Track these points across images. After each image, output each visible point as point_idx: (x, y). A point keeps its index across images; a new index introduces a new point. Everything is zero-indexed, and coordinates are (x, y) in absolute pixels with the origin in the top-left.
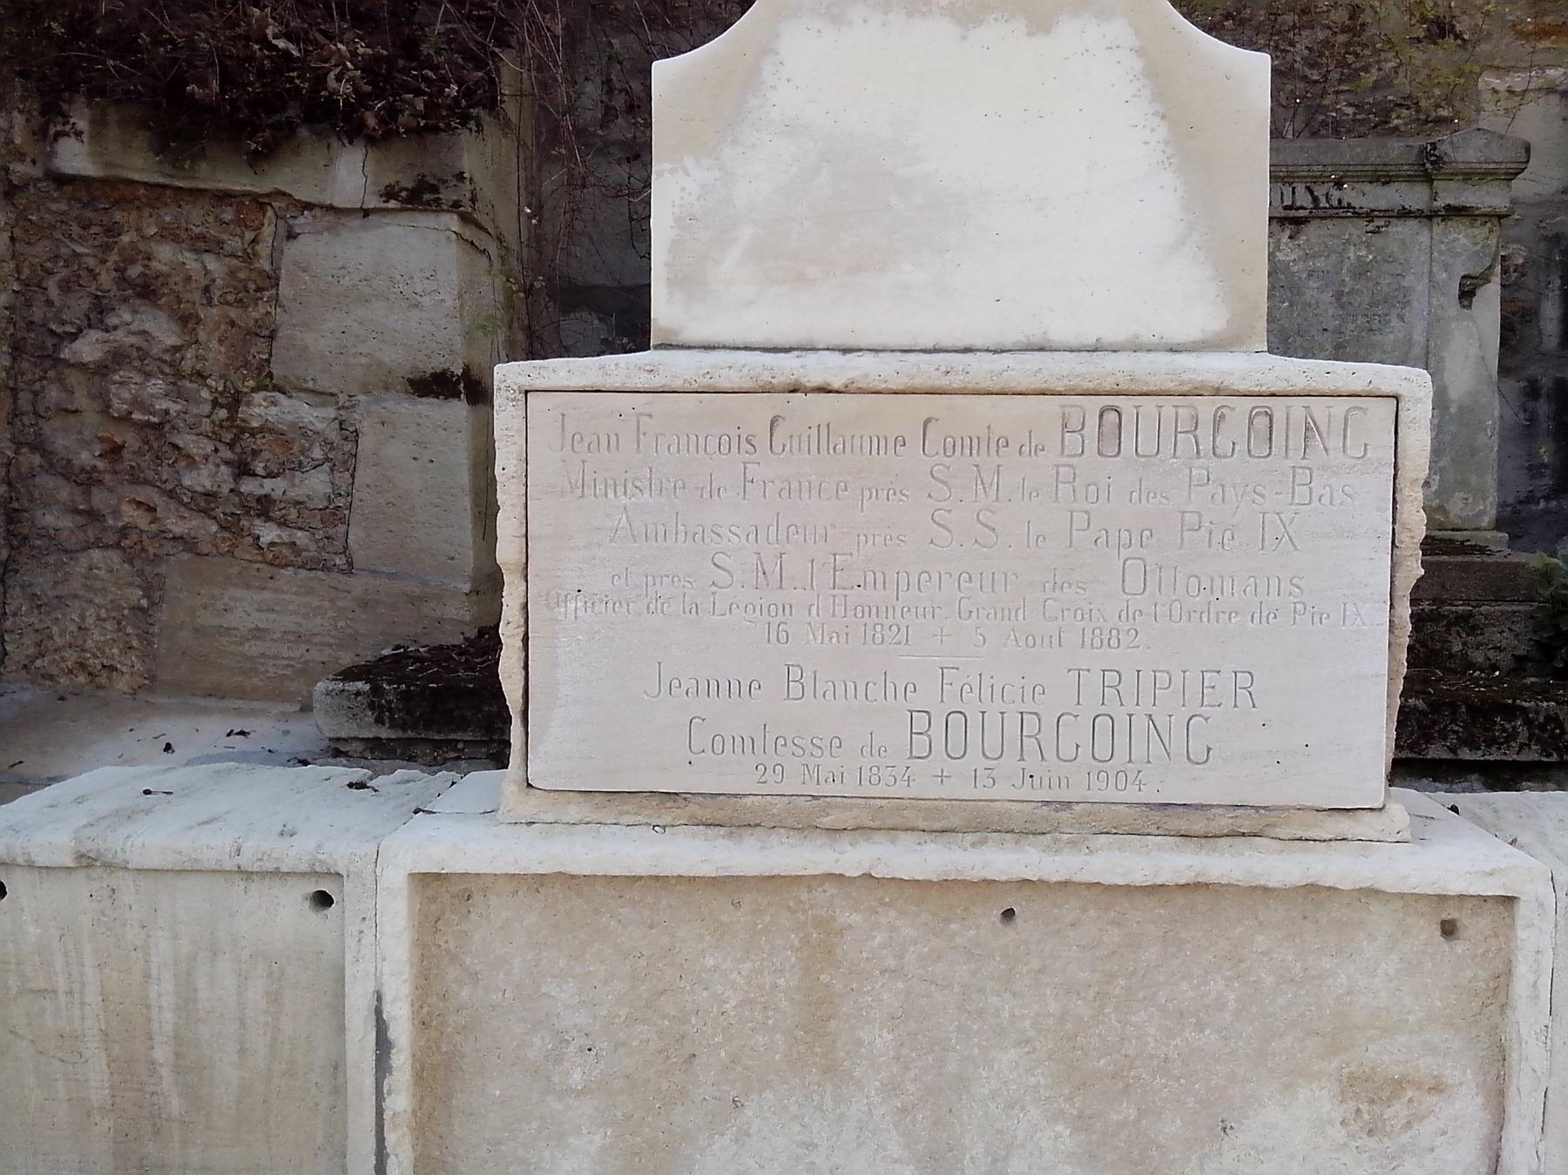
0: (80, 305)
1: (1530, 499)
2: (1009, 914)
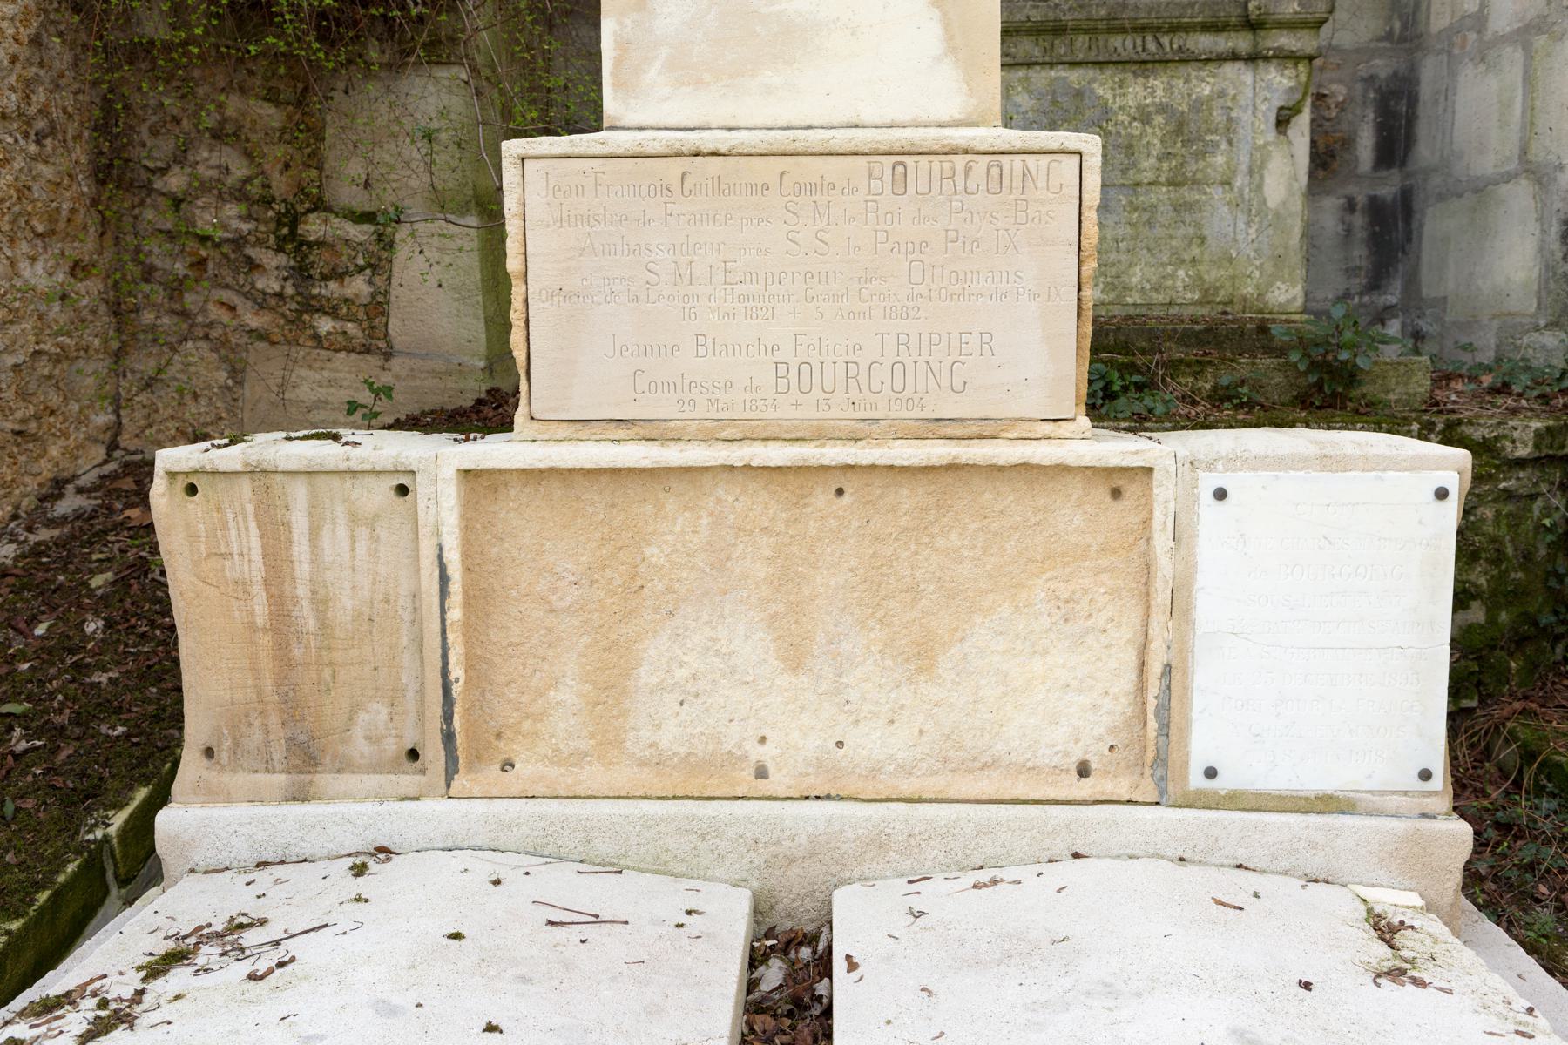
2: (840, 492)
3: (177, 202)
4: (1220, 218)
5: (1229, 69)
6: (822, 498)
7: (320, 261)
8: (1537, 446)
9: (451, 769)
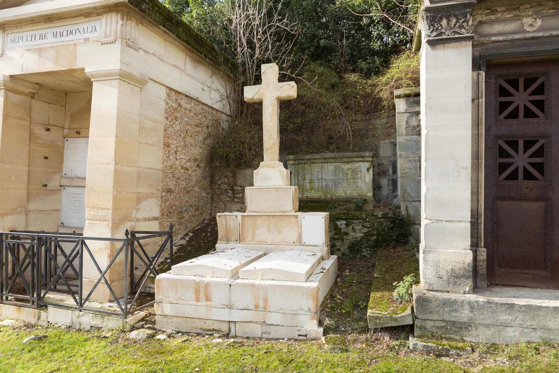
3: (219, 185)
4: (360, 184)
5: (360, 163)
6: (271, 218)
7: (236, 192)
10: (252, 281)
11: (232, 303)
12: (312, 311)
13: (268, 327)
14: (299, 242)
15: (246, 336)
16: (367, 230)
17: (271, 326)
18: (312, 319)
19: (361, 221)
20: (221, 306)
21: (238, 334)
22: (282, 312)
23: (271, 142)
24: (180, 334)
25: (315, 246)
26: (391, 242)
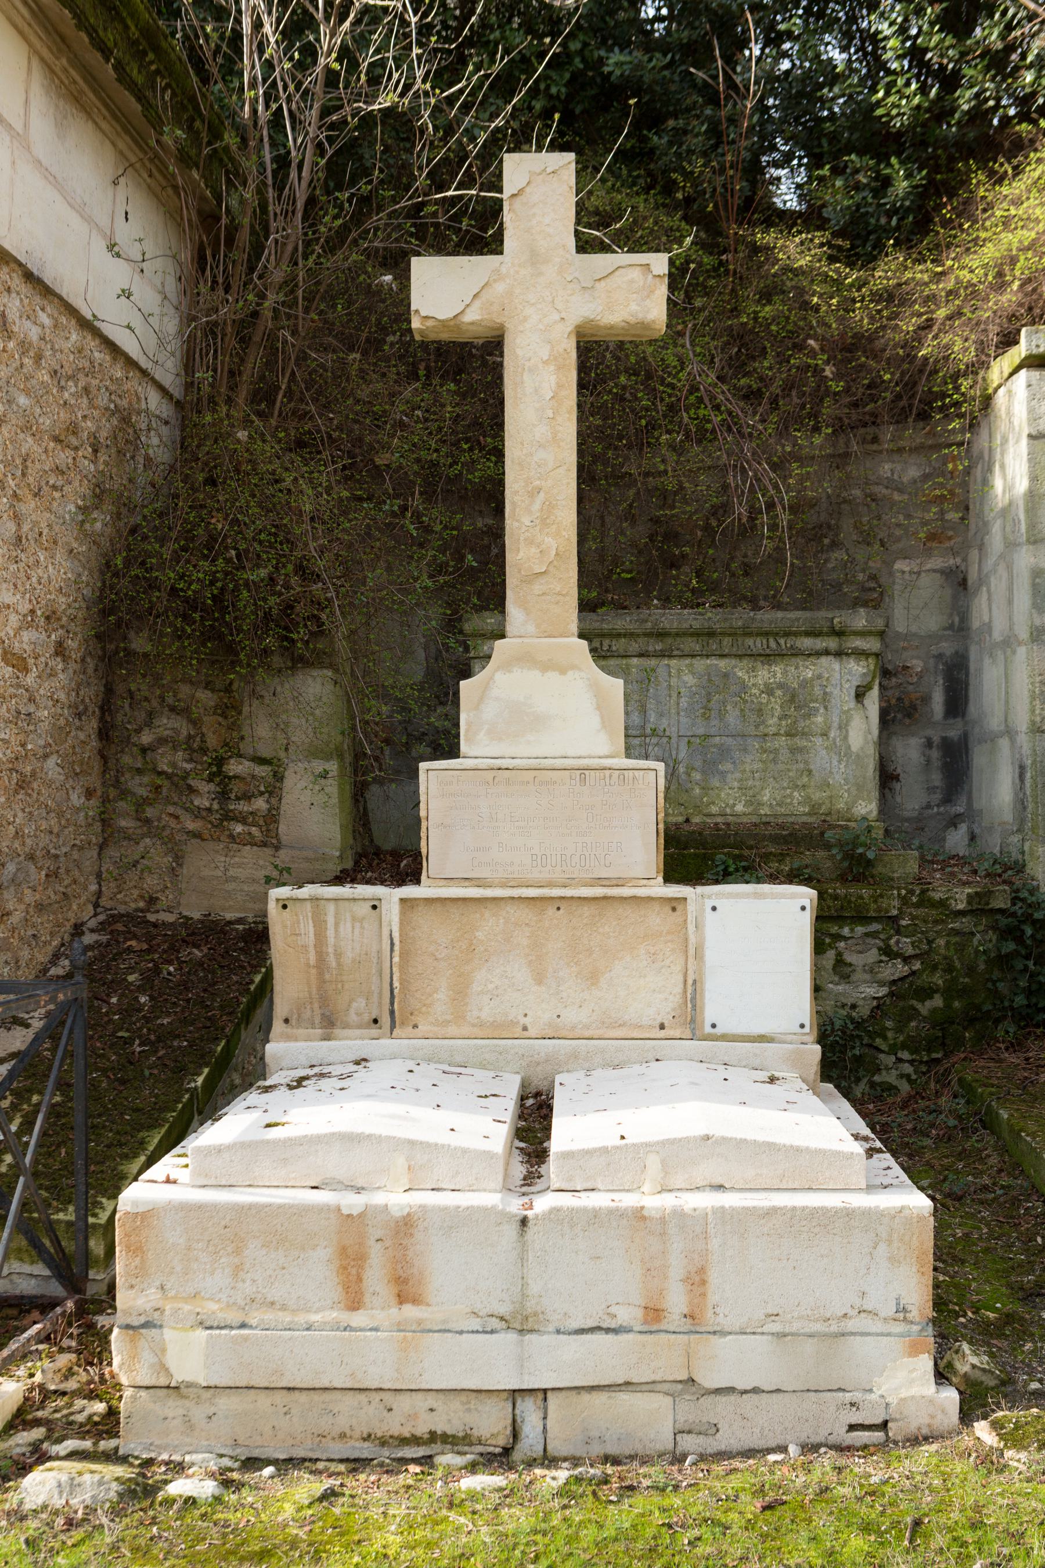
0: (141, 716)
1: (929, 806)
3: (144, 750)
4: (821, 758)
5: (824, 660)
6: (551, 911)
7: (236, 788)
8: (969, 903)
9: (393, 1026)
10: (629, 1200)
11: (531, 1306)
12: (914, 1314)
13: (707, 1401)
14: (690, 1020)
15: (597, 1450)
16: (900, 969)
17: (722, 1399)
18: (914, 1350)
19: (876, 927)
20: (475, 1324)
21: (556, 1447)
22: (776, 1327)
23: (551, 543)
24: (269, 1470)
25: (762, 1039)
26: (997, 1021)
